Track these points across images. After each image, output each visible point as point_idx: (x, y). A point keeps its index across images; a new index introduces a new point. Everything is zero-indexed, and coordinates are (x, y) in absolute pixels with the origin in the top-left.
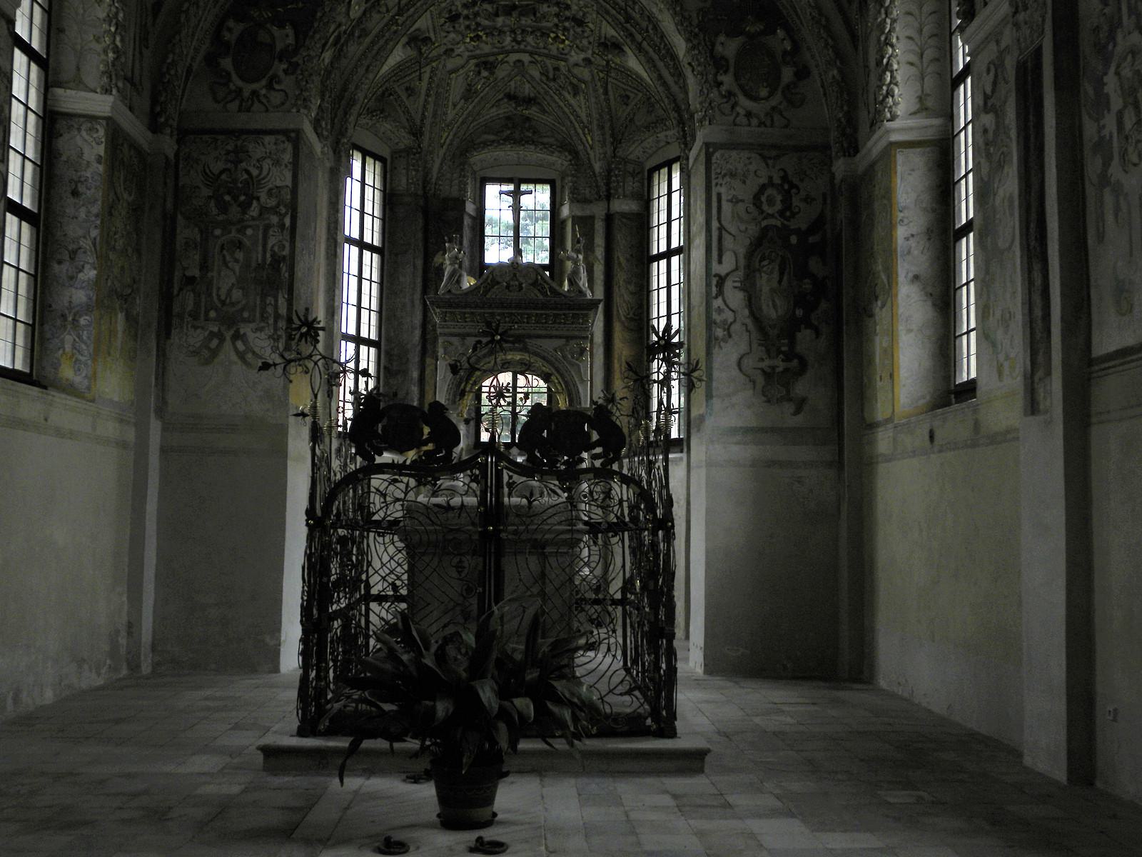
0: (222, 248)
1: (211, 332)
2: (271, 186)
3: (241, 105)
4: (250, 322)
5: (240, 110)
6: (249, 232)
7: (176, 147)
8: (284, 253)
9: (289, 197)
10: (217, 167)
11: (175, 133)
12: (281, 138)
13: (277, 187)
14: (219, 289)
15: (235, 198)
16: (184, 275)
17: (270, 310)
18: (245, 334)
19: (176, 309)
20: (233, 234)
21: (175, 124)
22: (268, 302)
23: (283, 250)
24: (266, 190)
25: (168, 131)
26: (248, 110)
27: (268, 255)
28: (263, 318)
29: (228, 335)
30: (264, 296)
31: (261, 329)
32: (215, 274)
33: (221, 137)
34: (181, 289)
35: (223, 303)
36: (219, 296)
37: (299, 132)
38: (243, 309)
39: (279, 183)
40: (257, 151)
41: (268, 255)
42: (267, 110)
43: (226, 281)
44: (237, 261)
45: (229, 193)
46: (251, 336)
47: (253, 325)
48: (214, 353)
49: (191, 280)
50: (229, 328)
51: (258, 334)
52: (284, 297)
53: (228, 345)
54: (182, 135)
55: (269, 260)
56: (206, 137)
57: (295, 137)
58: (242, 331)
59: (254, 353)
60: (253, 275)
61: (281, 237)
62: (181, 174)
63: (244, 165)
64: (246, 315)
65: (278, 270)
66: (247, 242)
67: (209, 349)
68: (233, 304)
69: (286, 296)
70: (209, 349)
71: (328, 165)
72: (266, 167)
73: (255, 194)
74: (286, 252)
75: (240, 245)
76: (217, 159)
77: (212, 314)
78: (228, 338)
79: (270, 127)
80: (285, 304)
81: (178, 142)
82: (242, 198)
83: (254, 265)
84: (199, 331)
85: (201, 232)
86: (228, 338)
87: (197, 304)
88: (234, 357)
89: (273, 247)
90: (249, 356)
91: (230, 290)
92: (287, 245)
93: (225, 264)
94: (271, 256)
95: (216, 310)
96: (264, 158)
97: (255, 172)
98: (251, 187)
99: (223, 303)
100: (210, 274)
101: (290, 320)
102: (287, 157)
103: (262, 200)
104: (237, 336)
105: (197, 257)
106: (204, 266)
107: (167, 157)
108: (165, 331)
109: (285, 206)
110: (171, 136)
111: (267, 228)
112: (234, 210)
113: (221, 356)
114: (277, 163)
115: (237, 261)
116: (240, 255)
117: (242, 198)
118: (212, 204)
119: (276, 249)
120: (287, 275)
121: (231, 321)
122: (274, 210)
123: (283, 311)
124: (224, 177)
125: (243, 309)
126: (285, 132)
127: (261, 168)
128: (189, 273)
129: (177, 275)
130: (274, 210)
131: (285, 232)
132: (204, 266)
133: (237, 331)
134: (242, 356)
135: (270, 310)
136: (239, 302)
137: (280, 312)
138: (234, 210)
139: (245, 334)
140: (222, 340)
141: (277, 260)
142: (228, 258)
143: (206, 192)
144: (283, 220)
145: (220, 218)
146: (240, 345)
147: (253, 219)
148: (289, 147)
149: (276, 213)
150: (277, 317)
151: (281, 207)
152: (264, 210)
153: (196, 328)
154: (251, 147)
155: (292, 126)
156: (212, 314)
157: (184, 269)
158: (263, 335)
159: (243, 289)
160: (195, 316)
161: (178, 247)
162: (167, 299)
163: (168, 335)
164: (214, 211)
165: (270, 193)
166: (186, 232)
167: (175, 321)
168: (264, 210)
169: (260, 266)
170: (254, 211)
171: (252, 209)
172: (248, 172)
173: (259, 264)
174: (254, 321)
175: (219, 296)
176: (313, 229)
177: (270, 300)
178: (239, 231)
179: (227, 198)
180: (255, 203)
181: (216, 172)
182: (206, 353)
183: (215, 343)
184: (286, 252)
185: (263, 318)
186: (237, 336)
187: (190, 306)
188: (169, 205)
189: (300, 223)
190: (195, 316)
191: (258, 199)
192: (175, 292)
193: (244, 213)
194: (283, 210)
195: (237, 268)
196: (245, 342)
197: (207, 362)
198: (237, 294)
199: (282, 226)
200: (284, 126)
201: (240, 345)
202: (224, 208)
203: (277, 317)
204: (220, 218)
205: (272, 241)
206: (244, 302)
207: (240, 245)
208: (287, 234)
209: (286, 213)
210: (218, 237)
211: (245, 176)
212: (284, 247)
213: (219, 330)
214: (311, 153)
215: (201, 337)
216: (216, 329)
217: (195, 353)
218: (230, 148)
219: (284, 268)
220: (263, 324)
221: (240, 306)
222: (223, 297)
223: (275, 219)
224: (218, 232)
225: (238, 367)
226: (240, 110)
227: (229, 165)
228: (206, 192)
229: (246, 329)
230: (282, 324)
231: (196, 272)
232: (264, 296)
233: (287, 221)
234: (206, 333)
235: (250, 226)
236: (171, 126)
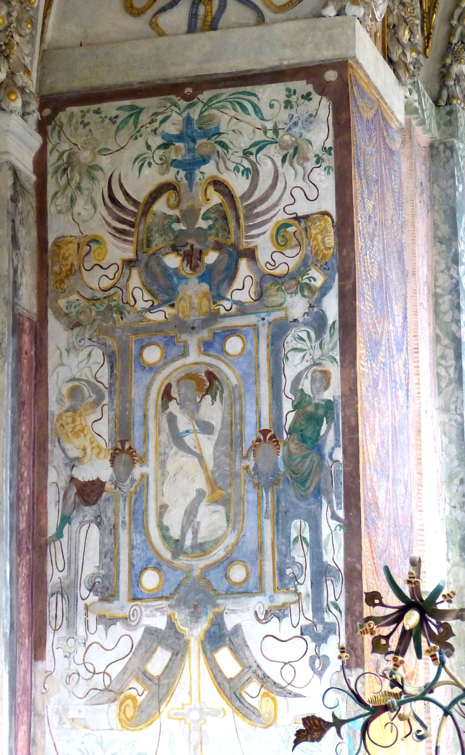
0: (167, 395)
1: (150, 632)
2: (281, 217)
3: (193, 16)
4: (247, 593)
5: (192, 29)
6: (234, 345)
7: (36, 141)
8: (328, 395)
9: (331, 240)
10: (141, 183)
11: (34, 105)
12: (302, 86)
13: (298, 218)
14: (163, 509)
15: (192, 258)
16: (72, 479)
17: (300, 555)
18: (237, 629)
19: (55, 576)
20: (194, 356)
21: (32, 86)
22: (294, 534)
23: (326, 388)
24: (270, 228)
25: (17, 103)
26: (213, 27)
27: (287, 406)
28: (284, 580)
29: (195, 633)
30: (281, 523)
31: (278, 612)
32: (150, 469)
33: (149, 104)
34: (65, 519)
35: (177, 547)
36: (163, 530)
37: (342, 65)
38: (228, 561)
39: (303, 208)
40: (238, 127)
41: (287, 406)
42: (261, 20)
43: (178, 485)
44: (206, 428)
45: (174, 249)
46: (253, 632)
47: (258, 603)
48: (161, 688)
49: (89, 493)
50: (196, 615)
51: (273, 626)
52: (334, 516)
53: (195, 663)
54: (52, 108)
55: (289, 418)
56: (110, 108)
57: (335, 84)
58: (230, 622)
59: (264, 679)
60: (251, 463)
61: (317, 353)
62: (52, 209)
63: (209, 170)
64: (238, 574)
65: (316, 444)
66: (230, 375)
67: (145, 676)
68: (201, 549)
69: (341, 514)
70: (145, 676)
71: (423, 137)
72: (266, 171)
73: (244, 244)
74: (333, 392)
75: (210, 383)
76: (141, 161)
77: (150, 580)
78: (195, 647)
79: (269, 60)
80: (341, 533)
81: (42, 127)
82: (211, 257)
83: (250, 434)
84: (118, 629)
85: (110, 358)
86: (195, 647)
87: (109, 554)
88: (213, 698)
89: (298, 379)
90: (254, 688)
91: (191, 513)
92: (335, 371)
93: (177, 439)
94: (295, 407)
95: (158, 568)
96: (261, 146)
97: (239, 185)
98: (232, 224)
99: (177, 547)
100: (137, 471)
101: (353, 575)
102: (320, 136)
103: (263, 256)
104: (217, 637)
105: (104, 428)
106: (124, 451)
107: (15, 173)
108: (33, 637)
109: (325, 268)
110: (24, 115)
111: (280, 330)
112: (193, 290)
113: (179, 697)
114: (294, 153)
115: (206, 428)
116: (213, 411)
117: (211, 257)
118: (135, 280)
119: (306, 385)
120: (339, 455)
121: (198, 594)
122: (293, 281)
123: (334, 554)
124: (161, 206)
125: (228, 561)
126: (310, 72)
127: (253, 173)
128: (85, 474)
129: (56, 477)
130: (293, 281)
131: (326, 336)
132: (124, 451)
133: (218, 621)
134: (231, 691)
135: (300, 555)
136: (217, 542)
137: (327, 558)
138: (193, 290)
139: (237, 629)
140: (179, 651)
141: (311, 416)
142: (184, 423)
143: (118, 251)
144: (319, 301)
145: (157, 317)
146: (224, 657)
147: (243, 309)
148: (323, 108)
149: (304, 288)
150: (321, 572)
151: (314, 273)
152: (267, 283)
153: (108, 621)
154: (224, 120)
155: (328, 54)
156: (150, 580)
157: (73, 463)
158: (285, 628)
159: (225, 502)
160: (107, 593)
161: (54, 407)
162: (33, 546)
163: (38, 649)
164: (142, 299)
165: (281, 237)
166: (73, 362)
167: (55, 607)
168: (267, 283)
169: (268, 437)
170: (243, 288)
171: (237, 284)
172: (220, 185)
173: (265, 432)
174: (260, 591)
175: (163, 530)
176: (399, 320)
177: (298, 527)
178: (206, 346)
179: (173, 261)
180: (243, 263)
181: (141, 197)
182: (137, 689)
183: (159, 661)
184: (333, 392)
185: (284, 580)
186: (217, 637)
187: (91, 564)
188: (28, 300)
189: (364, 306)
190: (107, 593)
191: (251, 254)
192: (52, 530)
193: (218, 297)
194: (317, 278)
195: (207, 445)
196: (239, 650)
197: (140, 717)
198: (211, 520)
199: (318, 323)
200: (308, 55)
201: (224, 657)
202: (164, 289)
203: (321, 572)
204: (157, 317)
205: (293, 366)
206: (231, 540)
207: (210, 383)
208: (332, 340)
209: (325, 290)
210: (153, 369)
211: (216, 198)
212: (326, 374)
213: (171, 624)
214: (381, 117)
215: (124, 647)
216: (160, 622)
217: (112, 693)
218: (172, 128)
219: (330, 436)
220: (282, 598)
221: (219, 553)
222: (175, 533)
223: (297, 306)
224: (152, 355)
225: (228, 720)
226: (192, 29)
227: (171, 175)
228: (118, 251)
229: (241, 616)
230: (335, 592)
231: (98, 469)
232: (281, 523)
233: (331, 306)
234: (138, 635)
235: (233, 331)
236: (22, 89)
